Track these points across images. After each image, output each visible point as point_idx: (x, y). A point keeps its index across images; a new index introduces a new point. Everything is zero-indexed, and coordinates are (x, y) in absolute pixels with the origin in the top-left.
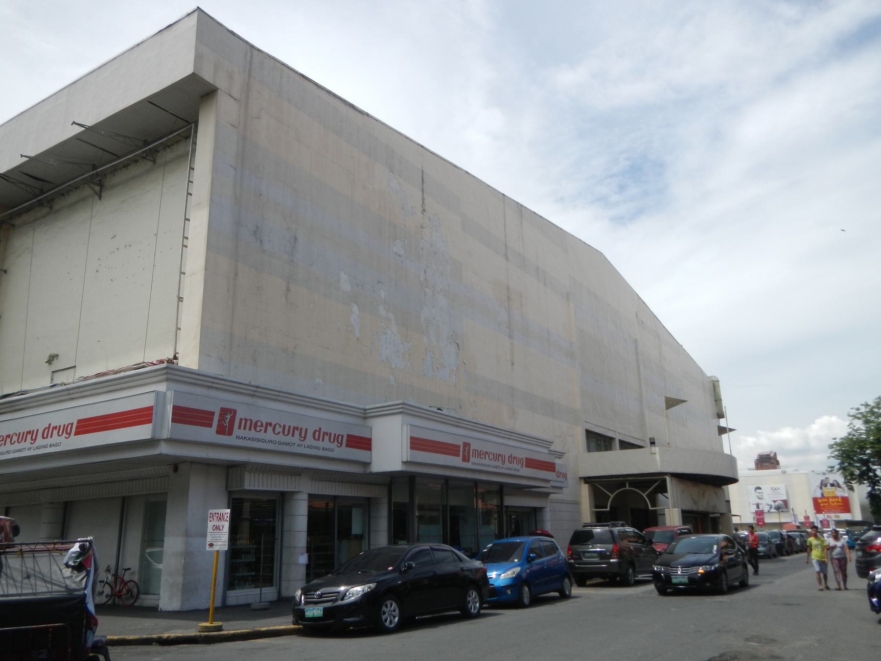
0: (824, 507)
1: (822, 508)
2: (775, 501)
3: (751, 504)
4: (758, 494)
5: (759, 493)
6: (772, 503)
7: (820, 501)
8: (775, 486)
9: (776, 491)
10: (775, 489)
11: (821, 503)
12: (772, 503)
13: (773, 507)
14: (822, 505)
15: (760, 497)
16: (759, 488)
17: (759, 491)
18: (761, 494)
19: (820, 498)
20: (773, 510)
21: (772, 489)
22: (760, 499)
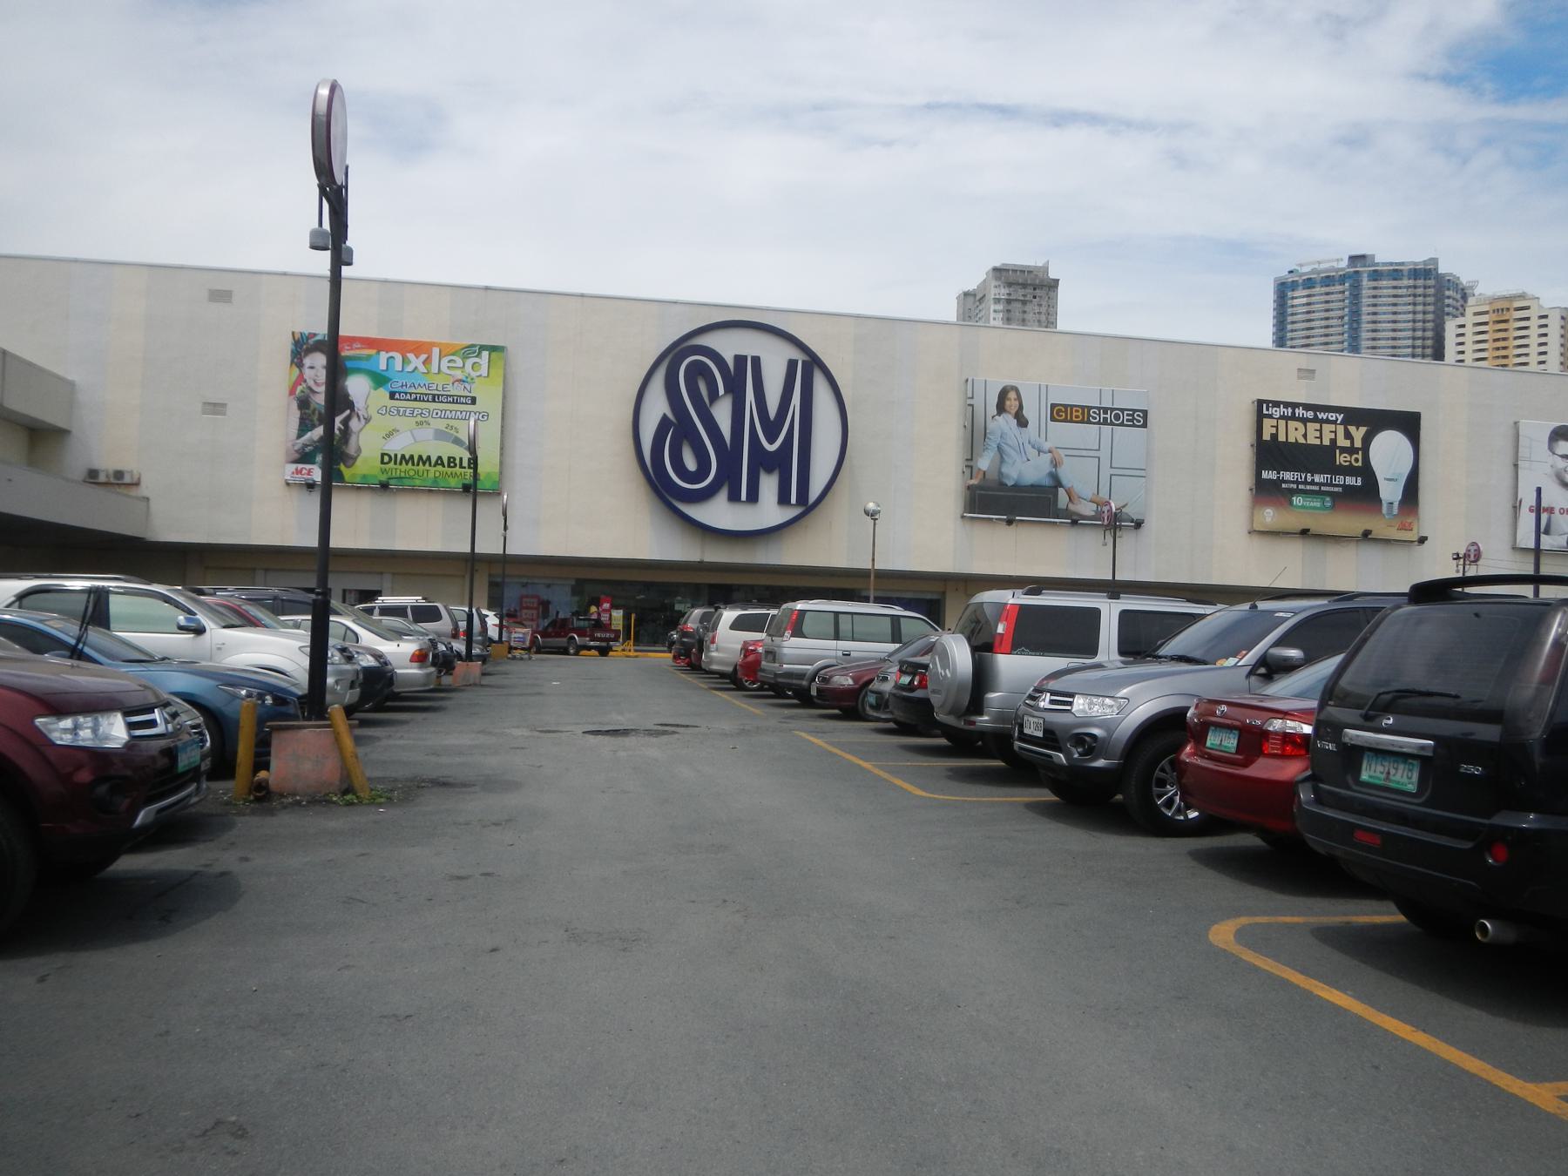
4: (1561, 464)
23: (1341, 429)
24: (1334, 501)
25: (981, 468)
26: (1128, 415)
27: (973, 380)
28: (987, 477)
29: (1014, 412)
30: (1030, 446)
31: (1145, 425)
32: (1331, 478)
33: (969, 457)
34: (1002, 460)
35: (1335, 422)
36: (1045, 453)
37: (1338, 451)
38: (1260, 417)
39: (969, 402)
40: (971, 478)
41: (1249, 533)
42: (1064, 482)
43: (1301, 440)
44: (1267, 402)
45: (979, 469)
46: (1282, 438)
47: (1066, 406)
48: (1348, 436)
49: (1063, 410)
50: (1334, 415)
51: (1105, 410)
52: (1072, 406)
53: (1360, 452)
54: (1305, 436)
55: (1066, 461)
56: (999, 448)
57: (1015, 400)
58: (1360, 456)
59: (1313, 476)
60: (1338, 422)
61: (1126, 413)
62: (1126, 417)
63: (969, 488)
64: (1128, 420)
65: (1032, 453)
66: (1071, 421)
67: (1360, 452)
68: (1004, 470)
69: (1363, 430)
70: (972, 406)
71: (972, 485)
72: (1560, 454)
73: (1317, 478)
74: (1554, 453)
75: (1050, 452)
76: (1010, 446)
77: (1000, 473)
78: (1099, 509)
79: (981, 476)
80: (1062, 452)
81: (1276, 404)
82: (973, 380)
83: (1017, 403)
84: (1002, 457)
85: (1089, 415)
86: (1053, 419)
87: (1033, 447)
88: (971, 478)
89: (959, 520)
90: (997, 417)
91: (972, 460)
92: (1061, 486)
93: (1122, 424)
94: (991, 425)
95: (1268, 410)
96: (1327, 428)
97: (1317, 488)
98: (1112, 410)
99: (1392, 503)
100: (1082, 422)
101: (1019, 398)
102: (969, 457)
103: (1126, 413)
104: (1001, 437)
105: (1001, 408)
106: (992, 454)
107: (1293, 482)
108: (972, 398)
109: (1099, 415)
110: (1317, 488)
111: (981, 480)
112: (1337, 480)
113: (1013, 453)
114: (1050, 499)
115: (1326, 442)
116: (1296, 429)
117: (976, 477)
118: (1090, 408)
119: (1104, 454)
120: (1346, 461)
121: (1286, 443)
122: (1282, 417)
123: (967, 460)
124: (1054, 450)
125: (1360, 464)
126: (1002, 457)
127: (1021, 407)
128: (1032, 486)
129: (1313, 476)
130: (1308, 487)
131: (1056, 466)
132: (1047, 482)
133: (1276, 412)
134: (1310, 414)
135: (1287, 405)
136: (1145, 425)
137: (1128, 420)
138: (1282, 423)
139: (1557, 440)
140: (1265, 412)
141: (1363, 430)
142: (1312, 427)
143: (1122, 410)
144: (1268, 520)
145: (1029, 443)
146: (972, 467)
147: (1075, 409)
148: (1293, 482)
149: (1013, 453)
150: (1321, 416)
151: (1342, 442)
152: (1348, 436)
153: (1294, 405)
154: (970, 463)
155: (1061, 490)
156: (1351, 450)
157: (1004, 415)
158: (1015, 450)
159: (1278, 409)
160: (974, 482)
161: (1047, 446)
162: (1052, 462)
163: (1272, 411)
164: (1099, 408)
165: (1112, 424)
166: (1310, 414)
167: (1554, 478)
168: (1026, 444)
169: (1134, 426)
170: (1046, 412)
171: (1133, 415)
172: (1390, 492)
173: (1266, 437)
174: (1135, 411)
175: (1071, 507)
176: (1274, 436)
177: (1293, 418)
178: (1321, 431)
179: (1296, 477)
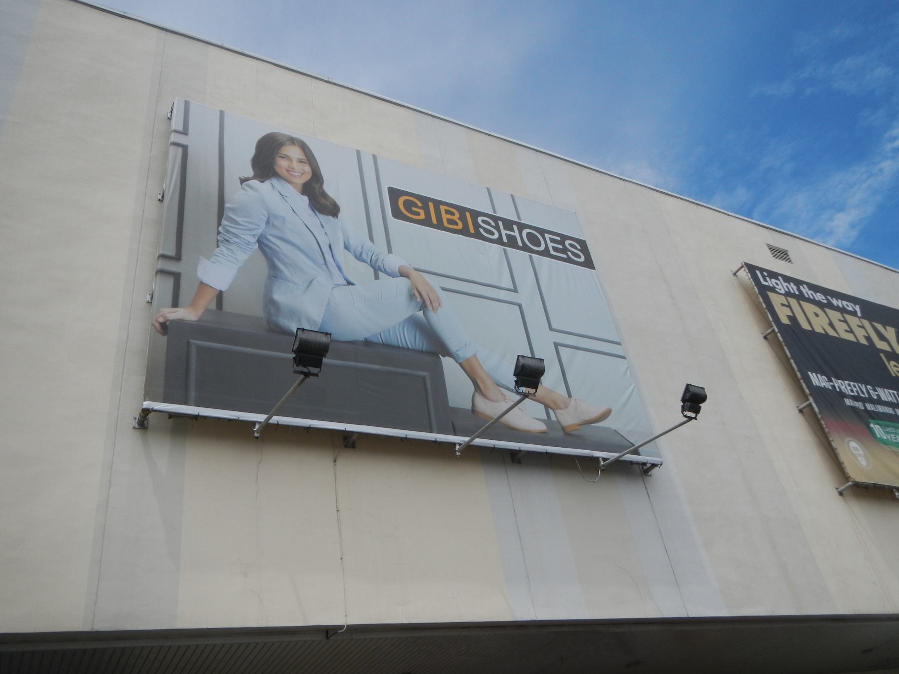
25: (206, 280)
26: (552, 240)
27: (187, 104)
28: (227, 307)
29: (301, 181)
30: (351, 257)
31: (589, 263)
33: (172, 253)
34: (274, 273)
35: (854, 313)
36: (391, 275)
37: (882, 355)
38: (764, 290)
39: (174, 138)
40: (175, 304)
41: (841, 494)
42: (453, 344)
43: (831, 333)
44: (762, 270)
45: (202, 285)
46: (805, 326)
47: (425, 200)
48: (882, 338)
49: (420, 204)
51: (508, 224)
52: (437, 203)
55: (443, 295)
56: (262, 243)
57: (301, 161)
59: (875, 390)
60: (859, 314)
61: (547, 236)
62: (550, 245)
63: (164, 327)
64: (555, 249)
65: (359, 271)
66: (440, 226)
68: (277, 297)
70: (185, 148)
71: (174, 322)
75: (403, 274)
76: (293, 244)
77: (270, 303)
78: (553, 418)
79: (207, 301)
80: (429, 278)
81: (773, 275)
82: (187, 104)
83: (307, 168)
84: (272, 266)
85: (477, 226)
86: (397, 214)
87: (359, 257)
88: (175, 304)
89: (130, 438)
90: (255, 183)
91: (178, 258)
92: (447, 353)
93: (546, 253)
94: (236, 195)
96: (853, 321)
97: (889, 410)
98: (522, 227)
100: (465, 232)
101: (309, 158)
102: (172, 253)
103: (547, 236)
104: (268, 223)
106: (242, 257)
107: (856, 398)
108: (185, 132)
109: (497, 227)
110: (889, 410)
111: (207, 311)
113: (301, 259)
114: (424, 378)
116: (817, 315)
117: (193, 304)
118: (475, 214)
119: (527, 294)
122: (788, 294)
123: (163, 257)
124: (414, 274)
126: (272, 266)
127: (316, 177)
128: (367, 343)
129: (875, 391)
130: (881, 409)
131: (423, 307)
132: (409, 339)
133: (782, 287)
134: (819, 297)
135: (787, 279)
136: (589, 263)
137: (555, 249)
138: (793, 302)
142: (835, 316)
143: (542, 232)
144: (864, 463)
145: (347, 248)
146: (177, 277)
147: (443, 208)
148: (856, 398)
149: (301, 259)
151: (881, 345)
152: (882, 338)
153: (798, 283)
154: (172, 267)
155: (446, 362)
157: (274, 181)
158: (314, 261)
159: (778, 282)
160: (185, 314)
161: (393, 262)
162: (412, 297)
163: (771, 282)
164: (496, 219)
166: (819, 297)
168: (339, 249)
169: (569, 260)
170: (379, 204)
171: (562, 242)
174: (564, 238)
175: (483, 405)
176: (793, 318)
177: (800, 297)
178: (845, 321)
179: (855, 389)
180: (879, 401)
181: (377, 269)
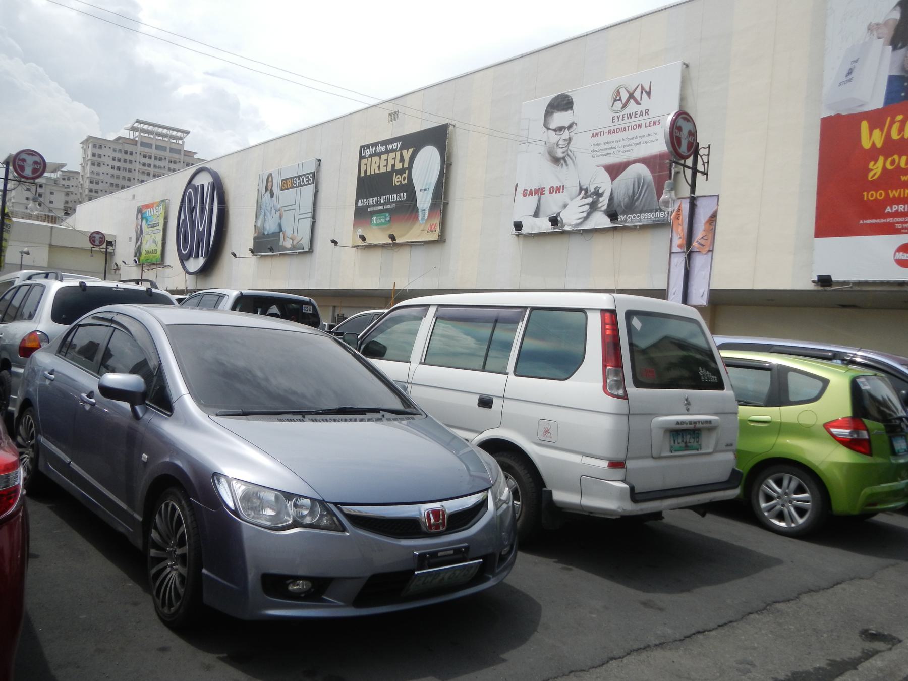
0: (890, 179)
1: (871, 196)
2: (615, 171)
3: (520, 190)
4: (553, 137)
5: (561, 129)
6: (605, 184)
7: (870, 138)
8: (631, 79)
9: (632, 107)
10: (631, 96)
11: (873, 154)
12: (605, 184)
13: (604, 202)
14: (876, 168)
15: (559, 153)
16: (563, 103)
17: (560, 118)
18: (566, 134)
19: (876, 119)
20: (600, 220)
21: (617, 98)
22: (556, 161)
23: (398, 153)
24: (390, 216)
32: (390, 197)
50: (396, 144)
53: (407, 171)
54: (379, 167)
58: (406, 175)
67: (407, 171)
69: (411, 150)
72: (554, 128)
73: (383, 199)
74: (548, 129)
75: (279, 210)
77: (264, 227)
80: (283, 209)
81: (367, 146)
95: (364, 153)
96: (392, 155)
99: (424, 210)
105: (266, 189)
112: (393, 198)
115: (389, 169)
116: (376, 163)
120: (398, 182)
121: (371, 175)
125: (406, 181)
128: (273, 233)
134: (383, 149)
139: (552, 113)
140: (363, 155)
141: (411, 150)
150: (390, 147)
153: (375, 145)
155: (281, 233)
156: (401, 172)
165: (302, 186)
167: (547, 155)
172: (424, 200)
173: (362, 174)
180: (381, 204)
181: (276, 211)
